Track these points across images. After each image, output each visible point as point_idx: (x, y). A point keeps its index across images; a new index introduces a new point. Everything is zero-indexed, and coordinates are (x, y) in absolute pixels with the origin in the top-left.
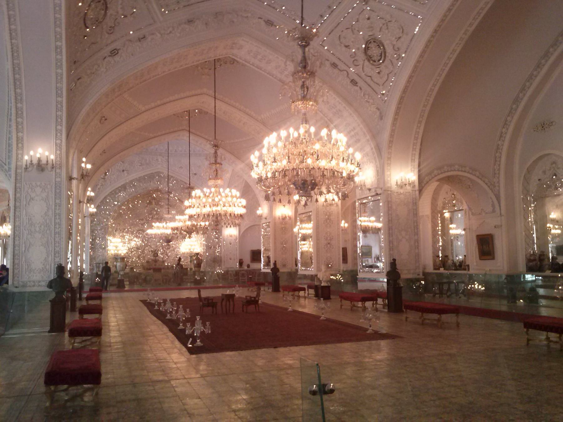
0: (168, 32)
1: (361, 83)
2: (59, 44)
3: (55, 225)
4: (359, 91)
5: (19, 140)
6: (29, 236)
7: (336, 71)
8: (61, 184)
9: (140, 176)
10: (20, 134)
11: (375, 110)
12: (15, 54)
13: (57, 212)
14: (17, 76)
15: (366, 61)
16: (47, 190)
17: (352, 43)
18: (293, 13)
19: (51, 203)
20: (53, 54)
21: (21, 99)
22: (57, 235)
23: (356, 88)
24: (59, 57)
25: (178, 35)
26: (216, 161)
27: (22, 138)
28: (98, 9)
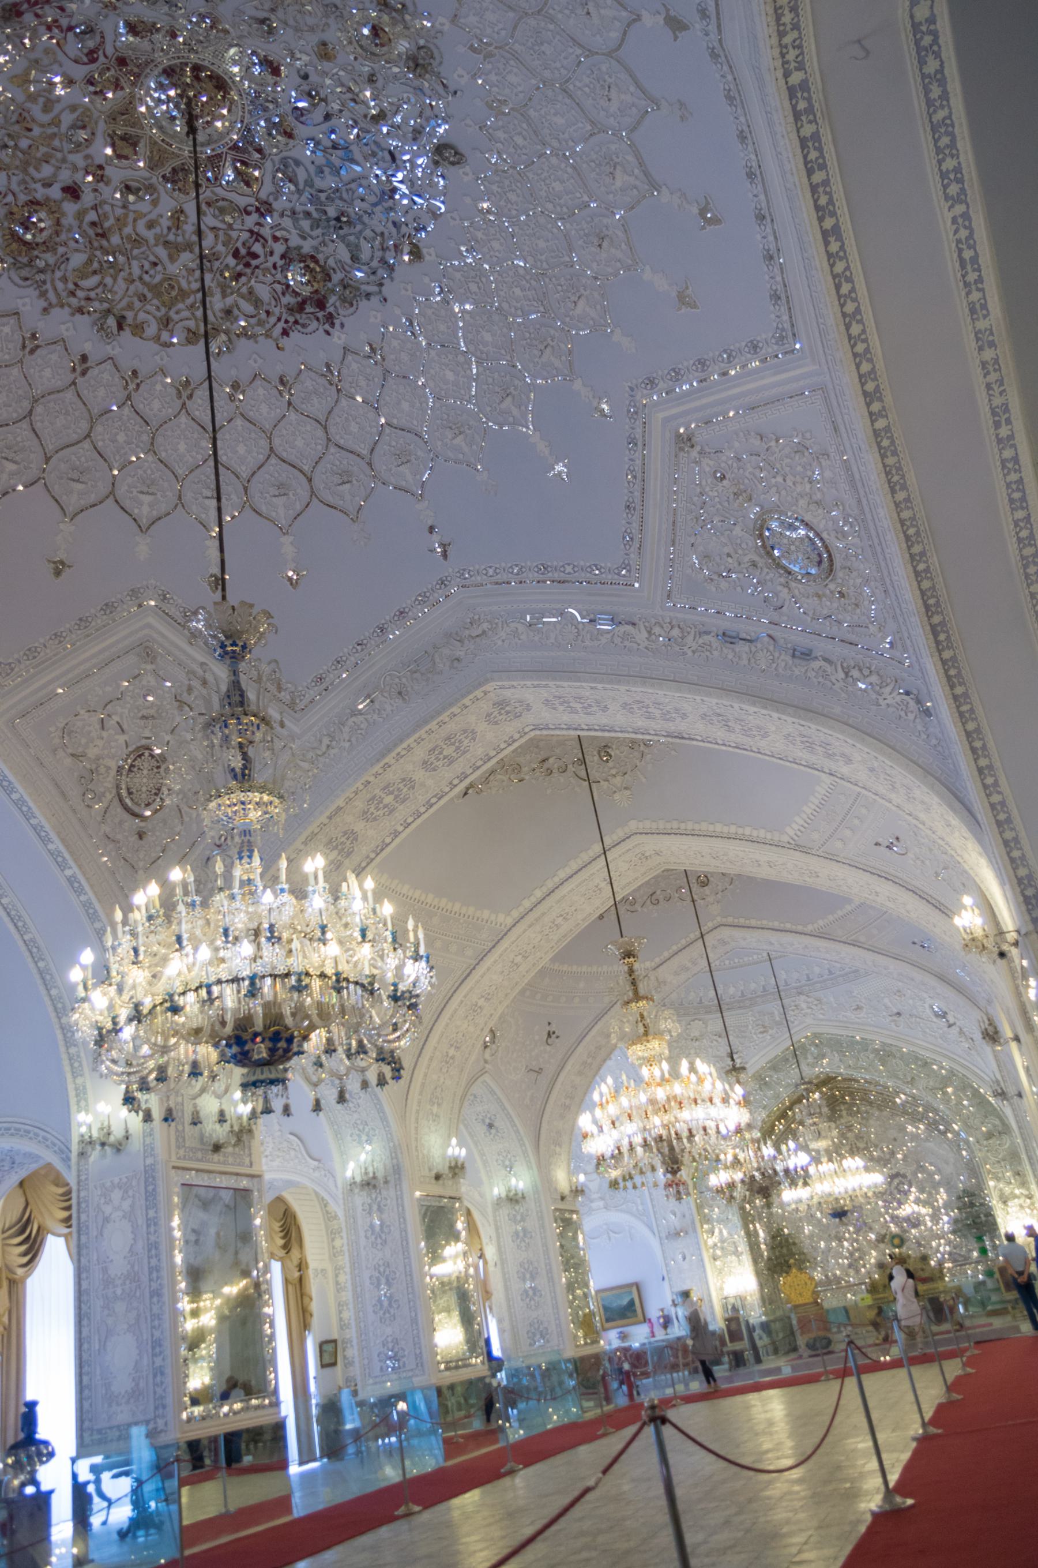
0: (324, 749)
1: (821, 647)
2: (68, 872)
3: (150, 1273)
4: (829, 669)
5: (81, 1093)
6: (106, 1312)
7: (742, 648)
8: (153, 1170)
9: (772, 1055)
10: (79, 1081)
11: (898, 698)
12: (20, 924)
13: (152, 1238)
14: (41, 964)
15: (793, 584)
16: (131, 1193)
17: (730, 560)
18: (569, 569)
19: (140, 1222)
20: (73, 896)
21: (64, 1008)
22: (155, 1299)
23: (816, 664)
24: (83, 898)
25: (347, 745)
26: (636, 992)
27: (84, 1087)
28: (145, 772)
